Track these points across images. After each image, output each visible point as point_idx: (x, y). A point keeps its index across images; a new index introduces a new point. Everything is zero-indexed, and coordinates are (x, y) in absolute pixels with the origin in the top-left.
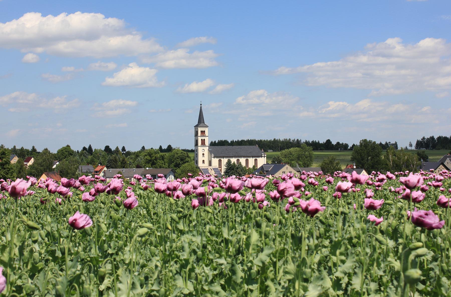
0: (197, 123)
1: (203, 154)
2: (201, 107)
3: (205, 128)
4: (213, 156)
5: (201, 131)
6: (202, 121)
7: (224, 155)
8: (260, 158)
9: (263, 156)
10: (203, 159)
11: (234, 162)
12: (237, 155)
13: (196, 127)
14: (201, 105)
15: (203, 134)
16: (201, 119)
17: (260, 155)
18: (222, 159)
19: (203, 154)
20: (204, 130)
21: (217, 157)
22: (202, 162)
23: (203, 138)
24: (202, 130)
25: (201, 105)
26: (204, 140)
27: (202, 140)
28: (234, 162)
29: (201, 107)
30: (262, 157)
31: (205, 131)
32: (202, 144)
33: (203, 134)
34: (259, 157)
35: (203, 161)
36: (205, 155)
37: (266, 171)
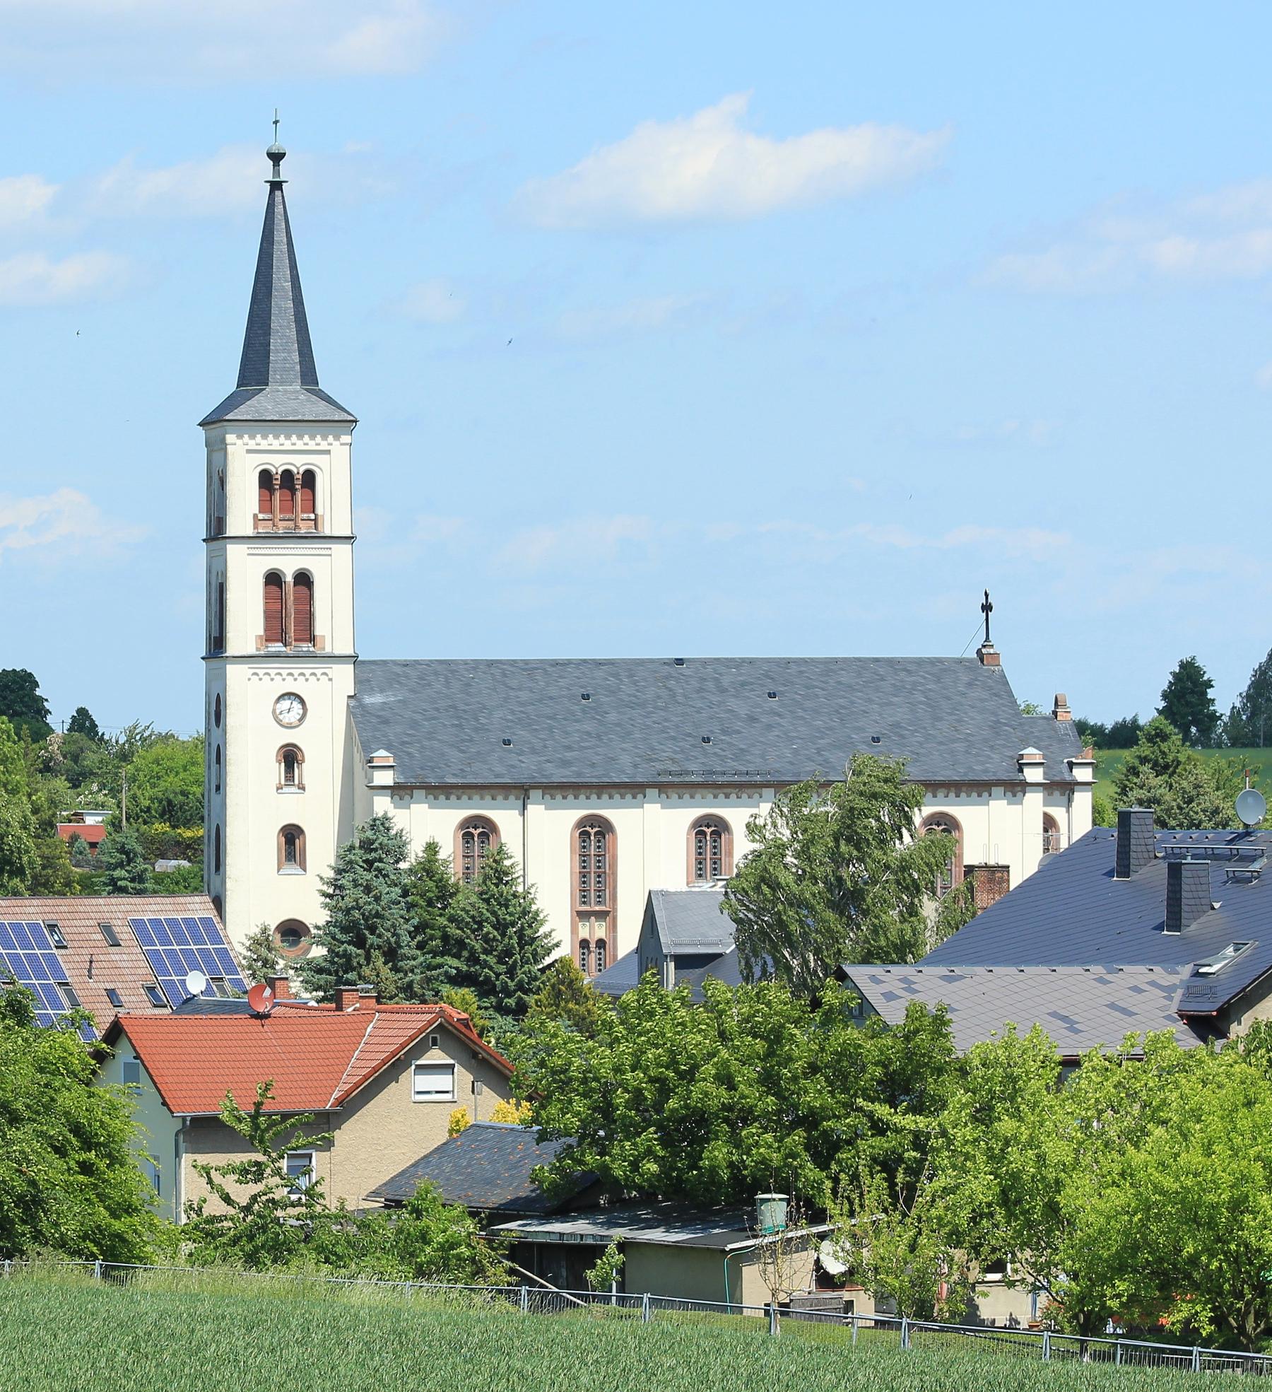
0: (231, 386)
1: (290, 757)
2: (276, 186)
3: (319, 443)
4: (385, 778)
5: (265, 478)
6: (282, 352)
7: (527, 767)
8: (999, 807)
9: (1034, 775)
10: (291, 809)
11: (432, 848)
12: (695, 768)
13: (216, 430)
14: (276, 157)
15: (289, 507)
16: (267, 333)
17: (998, 767)
18: (505, 819)
19: (290, 757)
20: (298, 464)
21: (441, 791)
22: (271, 844)
23: (289, 562)
24: (278, 464)
25: (276, 157)
26: (304, 579)
27: (273, 579)
28: (432, 848)
29: (276, 186)
30: (1016, 788)
31: (309, 478)
32: (275, 628)
33: (289, 507)
34: (979, 788)
35: (292, 837)
36: (308, 770)
37: (684, 962)
